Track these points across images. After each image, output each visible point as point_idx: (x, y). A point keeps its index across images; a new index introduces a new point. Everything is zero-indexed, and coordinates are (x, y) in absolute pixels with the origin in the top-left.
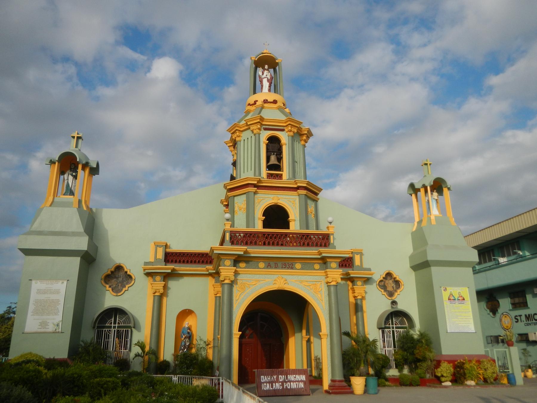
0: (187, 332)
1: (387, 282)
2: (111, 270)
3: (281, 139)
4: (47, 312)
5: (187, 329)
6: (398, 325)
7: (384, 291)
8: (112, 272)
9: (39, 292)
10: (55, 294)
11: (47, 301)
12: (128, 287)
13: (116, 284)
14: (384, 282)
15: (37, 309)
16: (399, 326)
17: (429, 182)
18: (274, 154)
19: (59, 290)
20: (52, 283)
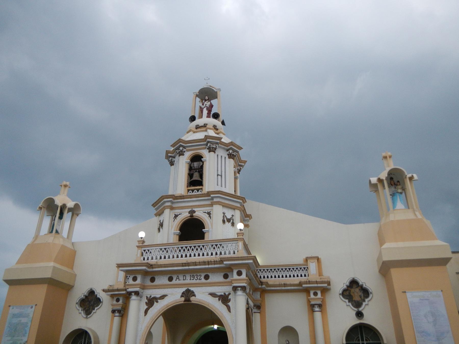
1: (352, 290)
2: (84, 294)
3: (203, 156)
6: (370, 341)
7: (349, 302)
8: (86, 297)
9: (14, 316)
13: (89, 307)
14: (349, 291)
16: (371, 342)
17: (384, 175)
18: (196, 172)
19: (29, 313)
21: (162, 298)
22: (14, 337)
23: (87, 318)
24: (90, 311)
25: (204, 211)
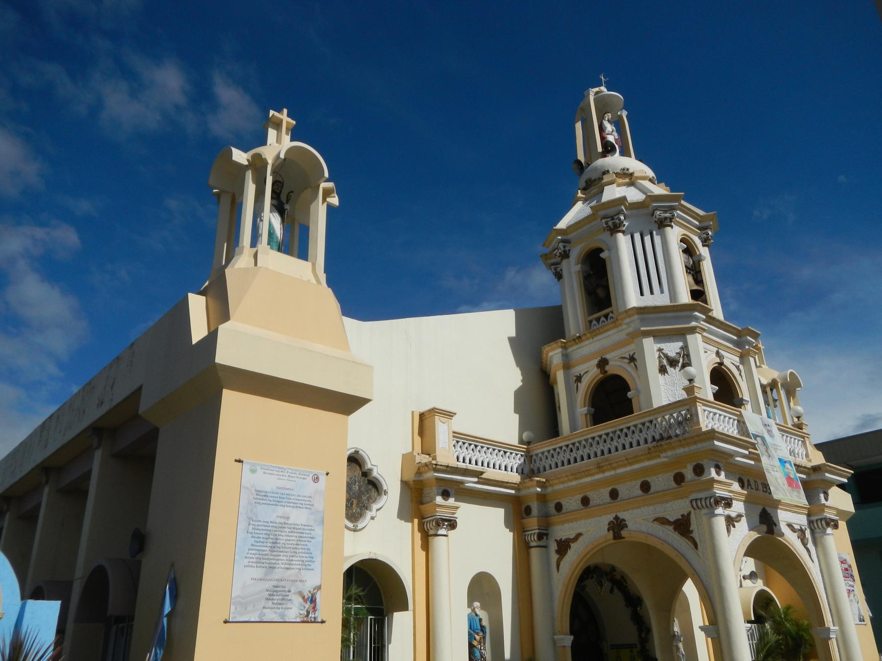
0: (479, 628)
4: (285, 558)
5: (478, 621)
9: (261, 495)
10: (300, 507)
11: (284, 526)
12: (378, 510)
15: (258, 548)
19: (310, 497)
20: (291, 477)
21: (738, 518)
22: (275, 570)
23: (355, 530)
24: (354, 511)
25: (733, 362)
